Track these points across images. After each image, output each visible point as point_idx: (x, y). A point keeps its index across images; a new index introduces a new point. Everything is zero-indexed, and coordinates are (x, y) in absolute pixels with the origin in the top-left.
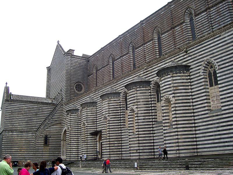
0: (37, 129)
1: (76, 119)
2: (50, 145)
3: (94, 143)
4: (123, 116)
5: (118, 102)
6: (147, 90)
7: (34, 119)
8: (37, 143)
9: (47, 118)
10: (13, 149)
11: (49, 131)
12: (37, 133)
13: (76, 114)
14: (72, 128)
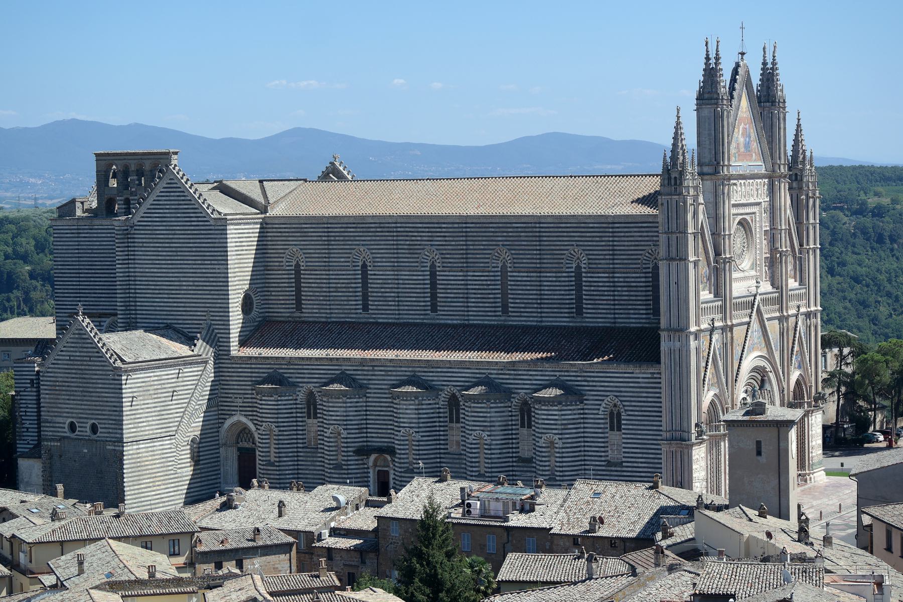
1: (291, 409)
2: (201, 462)
3: (361, 471)
4: (445, 433)
5: (434, 406)
6: (506, 407)
10: (142, 482)
14: (282, 429)
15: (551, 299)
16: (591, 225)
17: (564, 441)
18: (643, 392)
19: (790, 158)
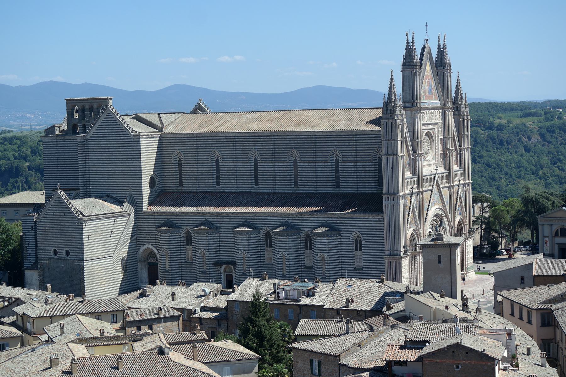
1: (177, 240)
2: (128, 271)
3: (217, 275)
4: (264, 253)
5: (257, 238)
6: (297, 238)
13: (177, 234)
14: (172, 252)
15: (322, 178)
16: (344, 136)
17: (330, 256)
18: (374, 229)
19: (454, 98)
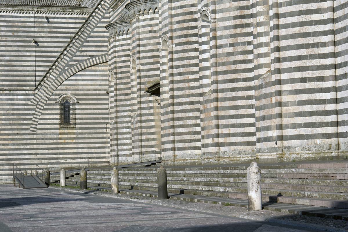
0: (38, 81)
2: (77, 126)
7: (28, 54)
8: (42, 122)
9: (65, 49)
11: (73, 88)
12: (39, 93)
14: (119, 76)
